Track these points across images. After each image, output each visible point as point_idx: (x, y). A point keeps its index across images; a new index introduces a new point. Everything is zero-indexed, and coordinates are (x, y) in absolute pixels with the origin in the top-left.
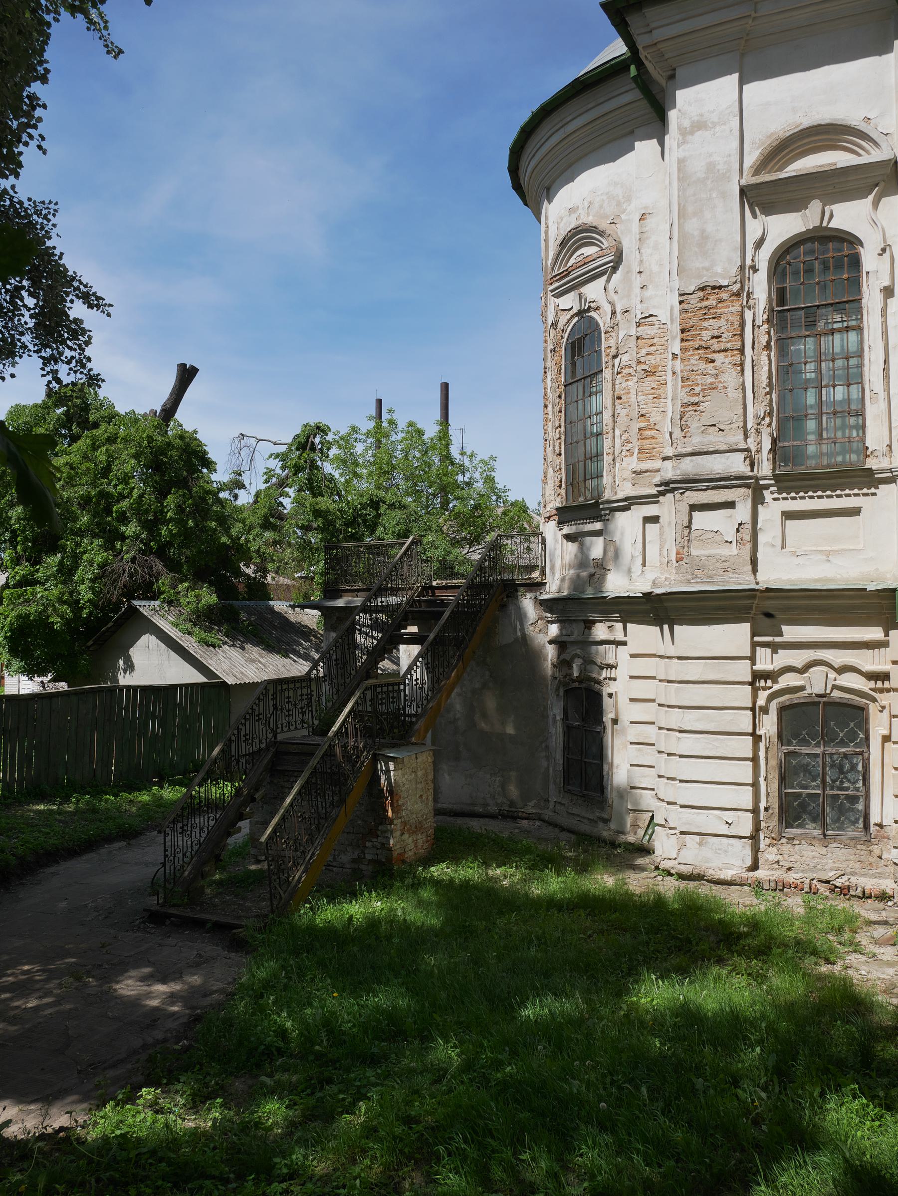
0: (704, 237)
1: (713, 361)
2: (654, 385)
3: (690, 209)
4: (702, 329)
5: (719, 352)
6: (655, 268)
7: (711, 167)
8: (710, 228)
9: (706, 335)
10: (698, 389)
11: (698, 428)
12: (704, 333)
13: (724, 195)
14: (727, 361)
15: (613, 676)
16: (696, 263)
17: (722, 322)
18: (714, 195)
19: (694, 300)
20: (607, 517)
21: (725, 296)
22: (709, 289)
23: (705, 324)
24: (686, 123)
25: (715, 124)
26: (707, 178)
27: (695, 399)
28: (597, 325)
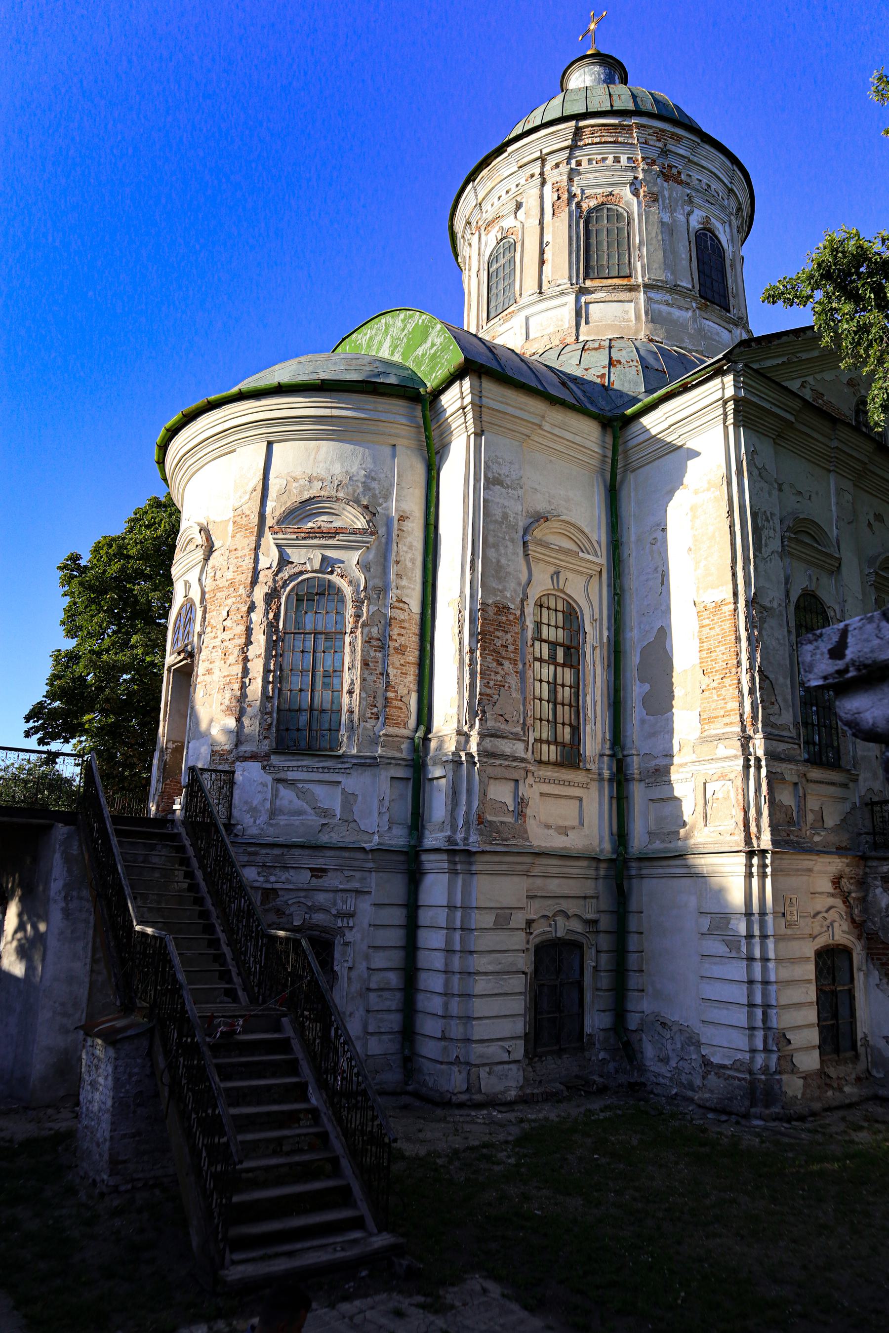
0: (499, 567)
1: (502, 665)
2: (402, 662)
3: (491, 540)
4: (495, 637)
5: (506, 658)
6: (409, 565)
7: (505, 516)
8: (503, 561)
9: (499, 643)
10: (492, 683)
11: (492, 715)
12: (496, 640)
13: (512, 540)
14: (511, 666)
15: (351, 924)
16: (494, 584)
17: (509, 636)
18: (507, 538)
19: (491, 611)
20: (348, 771)
21: (511, 617)
22: (502, 609)
23: (497, 633)
24: (490, 475)
25: (508, 487)
26: (502, 523)
27: (489, 691)
28: (339, 590)
